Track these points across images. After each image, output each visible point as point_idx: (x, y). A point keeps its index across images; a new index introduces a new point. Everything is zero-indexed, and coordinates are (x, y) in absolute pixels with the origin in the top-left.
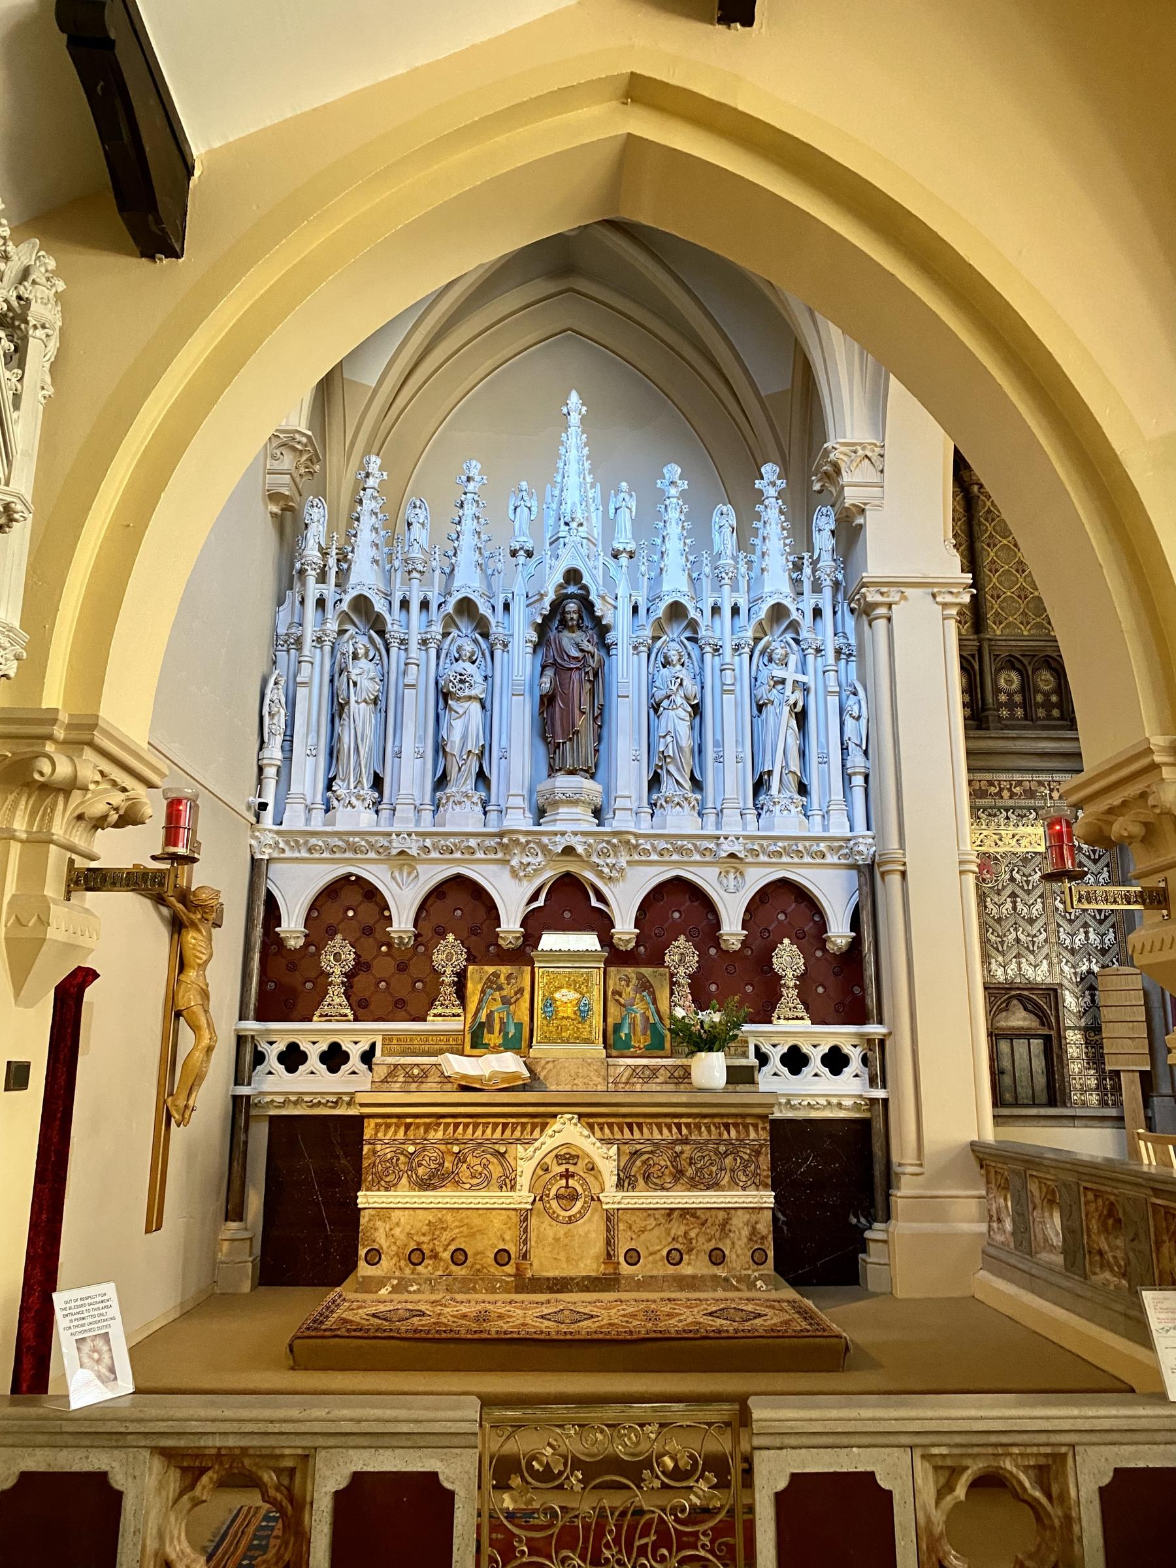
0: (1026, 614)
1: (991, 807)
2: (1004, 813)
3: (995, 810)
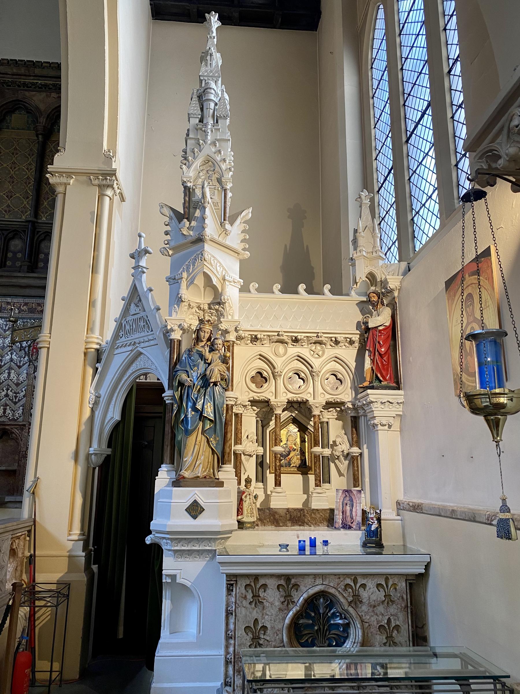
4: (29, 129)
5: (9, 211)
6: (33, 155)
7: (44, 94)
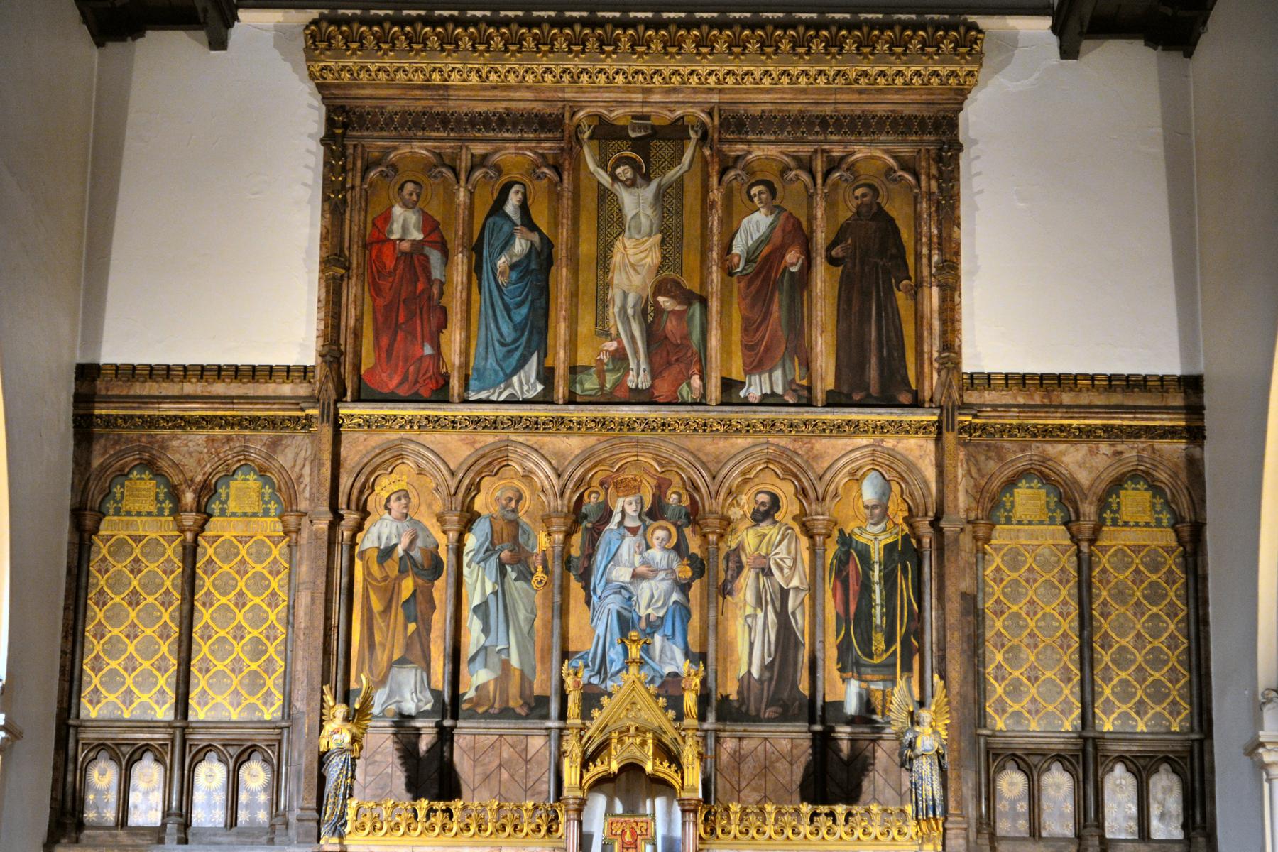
4: (1052, 521)
5: (1037, 711)
6: (1068, 581)
7: (1083, 449)
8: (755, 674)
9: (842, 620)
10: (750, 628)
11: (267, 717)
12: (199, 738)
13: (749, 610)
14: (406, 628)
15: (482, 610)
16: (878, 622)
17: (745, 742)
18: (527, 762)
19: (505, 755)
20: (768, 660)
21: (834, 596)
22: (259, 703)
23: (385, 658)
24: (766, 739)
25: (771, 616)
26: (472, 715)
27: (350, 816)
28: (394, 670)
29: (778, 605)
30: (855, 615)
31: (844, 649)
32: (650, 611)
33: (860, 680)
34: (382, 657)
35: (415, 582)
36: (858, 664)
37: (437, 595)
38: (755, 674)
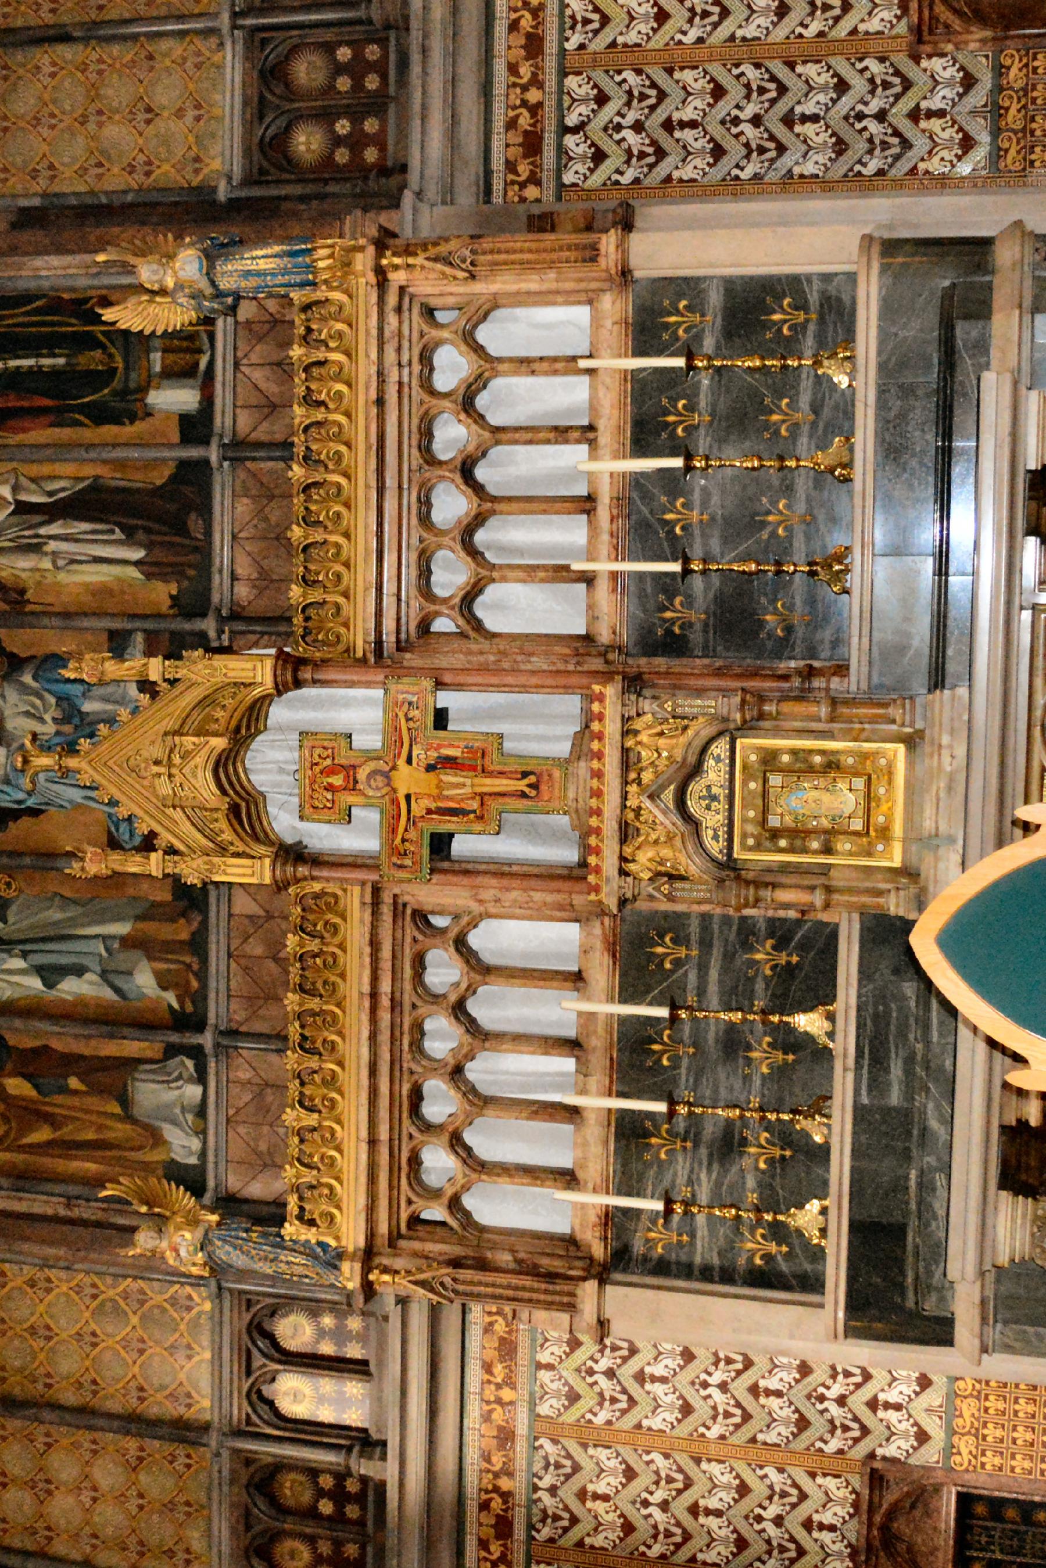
0: (172, 1346)
1: (529, 1516)
2: (540, 1493)
3: (535, 1511)
8: (139, 554)
9: (60, 417)
10: (73, 562)
11: (208, 1306)
12: (238, 1409)
13: (46, 564)
14: (76, 1092)
15: (51, 975)
16: (61, 361)
17: (240, 571)
18: (269, 917)
19: (259, 951)
20: (119, 535)
21: (24, 430)
22: (188, 1317)
23: (120, 1126)
24: (234, 537)
25: (55, 529)
26: (200, 997)
27: (310, 1235)
28: (136, 1112)
29: (38, 518)
30: (52, 398)
31: (101, 415)
32: (48, 717)
33: (143, 390)
34: (120, 1131)
35: (11, 1075)
36: (123, 393)
37: (30, 1043)
38: (139, 554)
